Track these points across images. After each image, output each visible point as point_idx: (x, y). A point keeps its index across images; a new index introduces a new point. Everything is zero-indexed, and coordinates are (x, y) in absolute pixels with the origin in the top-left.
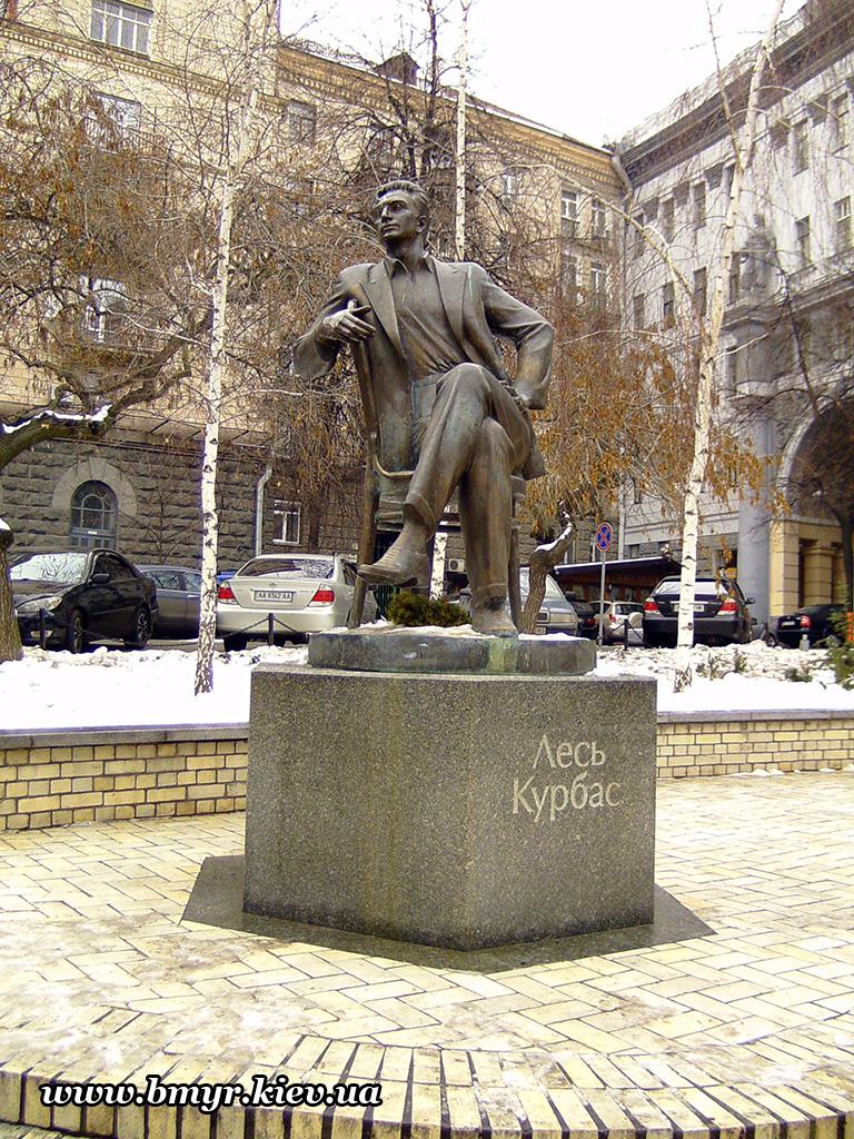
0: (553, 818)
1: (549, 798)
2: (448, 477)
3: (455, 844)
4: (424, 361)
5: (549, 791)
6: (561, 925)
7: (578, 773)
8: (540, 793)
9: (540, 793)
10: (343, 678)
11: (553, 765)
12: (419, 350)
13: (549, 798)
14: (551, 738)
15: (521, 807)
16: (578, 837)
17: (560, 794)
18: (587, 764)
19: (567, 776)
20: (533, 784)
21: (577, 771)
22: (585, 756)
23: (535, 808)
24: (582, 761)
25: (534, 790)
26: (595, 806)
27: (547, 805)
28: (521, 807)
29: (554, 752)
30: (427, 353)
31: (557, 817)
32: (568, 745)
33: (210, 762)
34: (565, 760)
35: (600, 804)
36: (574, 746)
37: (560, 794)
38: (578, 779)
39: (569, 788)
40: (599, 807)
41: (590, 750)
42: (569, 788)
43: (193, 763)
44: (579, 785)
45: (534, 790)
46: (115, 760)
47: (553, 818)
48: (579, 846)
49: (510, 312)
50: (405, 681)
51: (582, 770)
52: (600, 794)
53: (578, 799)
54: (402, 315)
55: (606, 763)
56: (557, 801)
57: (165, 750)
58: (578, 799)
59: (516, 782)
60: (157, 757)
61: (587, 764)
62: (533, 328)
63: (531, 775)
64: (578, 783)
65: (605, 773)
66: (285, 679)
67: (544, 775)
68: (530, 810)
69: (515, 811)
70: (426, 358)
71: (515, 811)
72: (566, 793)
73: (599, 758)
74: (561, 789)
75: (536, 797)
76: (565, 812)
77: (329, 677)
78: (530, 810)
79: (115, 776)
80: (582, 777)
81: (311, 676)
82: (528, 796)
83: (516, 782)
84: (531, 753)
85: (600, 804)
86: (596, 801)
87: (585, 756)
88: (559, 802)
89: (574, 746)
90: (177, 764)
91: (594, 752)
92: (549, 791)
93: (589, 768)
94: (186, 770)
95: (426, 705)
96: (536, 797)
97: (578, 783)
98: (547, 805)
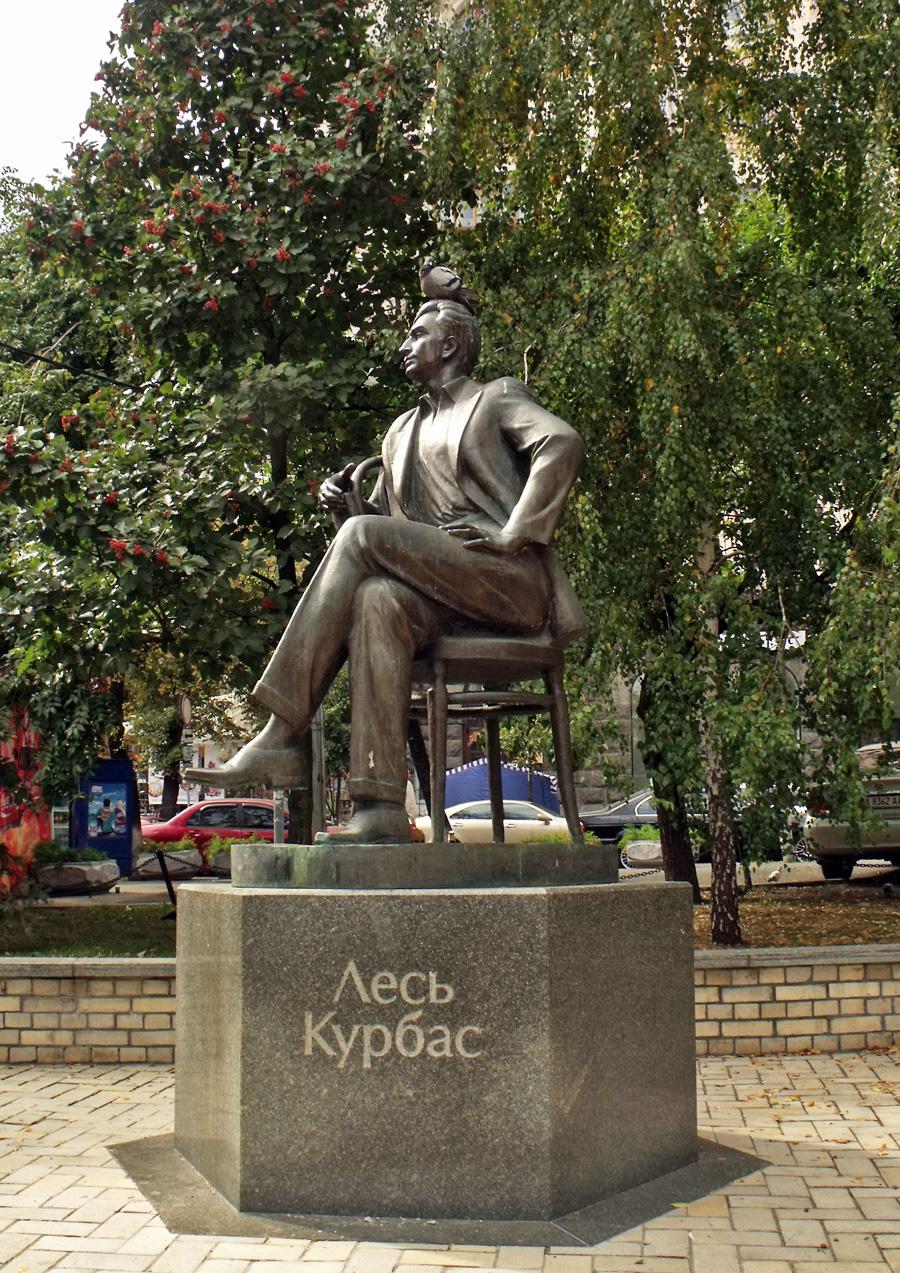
0: (367, 1065)
1: (360, 1039)
5: (361, 1032)
6: (385, 1202)
7: (407, 1012)
8: (347, 1032)
9: (347, 1032)
11: (365, 998)
13: (360, 1039)
14: (361, 968)
15: (316, 1049)
16: (410, 1093)
18: (422, 1000)
19: (391, 1014)
20: (335, 1020)
21: (404, 1009)
22: (418, 989)
23: (337, 1049)
24: (413, 997)
25: (336, 1029)
26: (436, 1055)
27: (358, 1050)
28: (316, 1049)
29: (367, 983)
31: (373, 1064)
32: (390, 976)
34: (386, 994)
35: (447, 1052)
36: (399, 977)
38: (407, 1018)
39: (393, 1029)
40: (443, 1060)
41: (427, 983)
42: (393, 1029)
44: (410, 1027)
47: (367, 1065)
48: (411, 1104)
51: (413, 1008)
52: (447, 1040)
55: (453, 1002)
56: (372, 1044)
59: (309, 1018)
61: (422, 1000)
63: (333, 1010)
64: (407, 1024)
65: (452, 1015)
67: (351, 1012)
68: (330, 1052)
69: (308, 1051)
71: (308, 1051)
72: (388, 1035)
73: (442, 993)
74: (380, 1032)
75: (339, 1036)
76: (387, 1058)
78: (330, 1052)
80: (415, 1016)
82: (327, 1033)
83: (309, 1018)
84: (332, 982)
85: (447, 1052)
86: (439, 1048)
87: (418, 989)
89: (399, 977)
91: (434, 986)
92: (361, 1032)
93: (427, 1006)
96: (339, 1036)
97: (407, 1024)
98: (358, 1050)
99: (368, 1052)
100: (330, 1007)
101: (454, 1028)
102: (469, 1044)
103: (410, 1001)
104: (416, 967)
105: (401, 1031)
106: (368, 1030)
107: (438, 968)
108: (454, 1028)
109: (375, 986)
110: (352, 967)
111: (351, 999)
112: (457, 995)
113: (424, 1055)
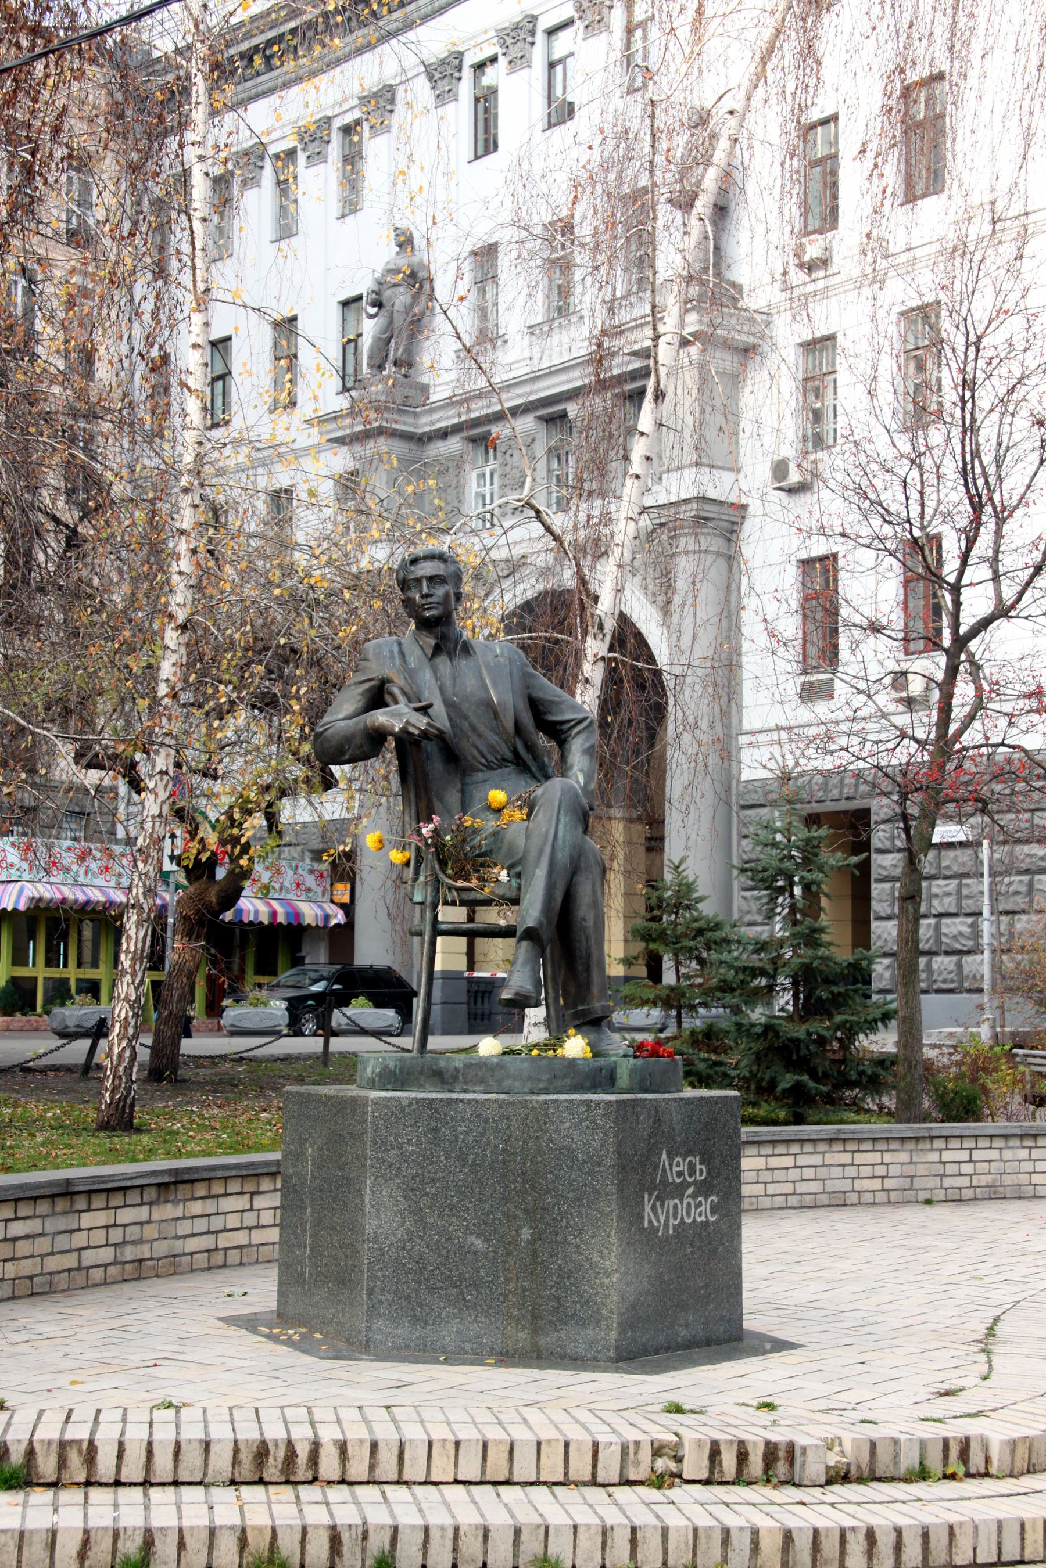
2: (559, 896)
3: (602, 1258)
4: (474, 757)
8: (662, 1206)
9: (662, 1206)
10: (477, 1101)
12: (470, 748)
14: (669, 1154)
15: (650, 1221)
17: (675, 1206)
19: (678, 1191)
20: (658, 1198)
21: (685, 1185)
23: (658, 1221)
24: (690, 1176)
26: (699, 1219)
27: (667, 1218)
28: (650, 1221)
29: (671, 1165)
30: (477, 748)
33: (101, 1218)
34: (680, 1174)
35: (703, 1218)
37: (675, 1206)
43: (87, 1220)
45: (658, 1204)
46: (17, 1219)
49: (552, 702)
50: (545, 1102)
51: (689, 1185)
53: (688, 1214)
54: (448, 704)
57: (61, 1205)
58: (688, 1214)
60: (54, 1214)
62: (580, 722)
65: (704, 1189)
66: (410, 1104)
68: (656, 1224)
69: (646, 1224)
70: (476, 753)
71: (646, 1224)
76: (679, 1225)
77: (462, 1101)
79: (15, 1239)
80: (690, 1191)
81: (441, 1100)
82: (654, 1208)
84: (656, 1167)
86: (700, 1215)
88: (675, 1218)
90: (71, 1222)
91: (698, 1167)
93: (695, 1182)
94: (79, 1230)
95: (568, 1124)
98: (667, 1218)
99: (672, 1222)
100: (655, 1188)
101: (706, 1199)
102: (714, 1209)
103: (689, 1179)
104: (689, 1152)
105: (685, 1202)
106: (672, 1203)
107: (700, 1153)
108: (706, 1199)
109: (675, 1169)
110: (664, 1156)
111: (664, 1181)
112: (708, 1173)
113: (694, 1220)
